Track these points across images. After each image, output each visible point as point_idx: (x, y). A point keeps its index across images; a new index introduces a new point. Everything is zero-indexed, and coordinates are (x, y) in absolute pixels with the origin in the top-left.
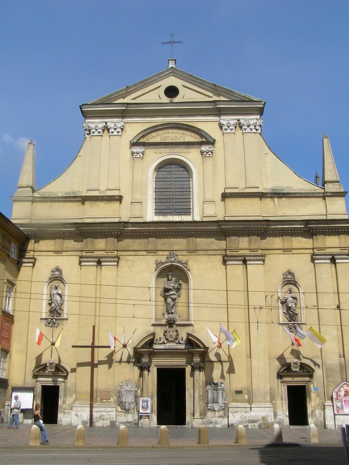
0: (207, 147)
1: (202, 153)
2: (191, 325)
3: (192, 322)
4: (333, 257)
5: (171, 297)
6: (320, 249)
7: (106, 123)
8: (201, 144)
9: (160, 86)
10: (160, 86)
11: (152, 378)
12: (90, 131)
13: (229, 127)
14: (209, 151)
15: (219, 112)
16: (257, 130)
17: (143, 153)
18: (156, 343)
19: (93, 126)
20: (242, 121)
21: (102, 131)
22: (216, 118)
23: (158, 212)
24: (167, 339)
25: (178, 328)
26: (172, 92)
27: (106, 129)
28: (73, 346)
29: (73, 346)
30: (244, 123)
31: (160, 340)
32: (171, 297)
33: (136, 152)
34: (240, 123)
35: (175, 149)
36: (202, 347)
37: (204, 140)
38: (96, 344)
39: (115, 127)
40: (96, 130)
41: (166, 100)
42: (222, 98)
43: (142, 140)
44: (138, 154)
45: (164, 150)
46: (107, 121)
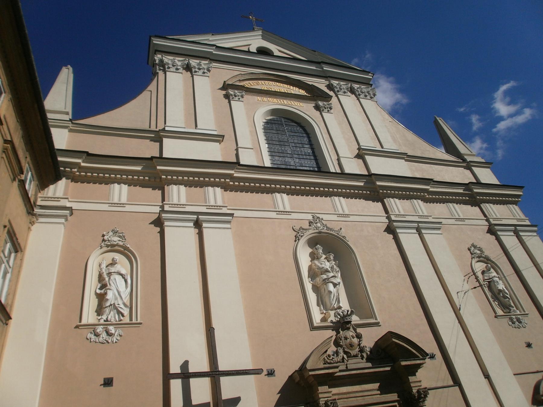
3: (379, 320)
5: (332, 282)
18: (329, 361)
24: (345, 352)
25: (359, 330)
32: (332, 282)
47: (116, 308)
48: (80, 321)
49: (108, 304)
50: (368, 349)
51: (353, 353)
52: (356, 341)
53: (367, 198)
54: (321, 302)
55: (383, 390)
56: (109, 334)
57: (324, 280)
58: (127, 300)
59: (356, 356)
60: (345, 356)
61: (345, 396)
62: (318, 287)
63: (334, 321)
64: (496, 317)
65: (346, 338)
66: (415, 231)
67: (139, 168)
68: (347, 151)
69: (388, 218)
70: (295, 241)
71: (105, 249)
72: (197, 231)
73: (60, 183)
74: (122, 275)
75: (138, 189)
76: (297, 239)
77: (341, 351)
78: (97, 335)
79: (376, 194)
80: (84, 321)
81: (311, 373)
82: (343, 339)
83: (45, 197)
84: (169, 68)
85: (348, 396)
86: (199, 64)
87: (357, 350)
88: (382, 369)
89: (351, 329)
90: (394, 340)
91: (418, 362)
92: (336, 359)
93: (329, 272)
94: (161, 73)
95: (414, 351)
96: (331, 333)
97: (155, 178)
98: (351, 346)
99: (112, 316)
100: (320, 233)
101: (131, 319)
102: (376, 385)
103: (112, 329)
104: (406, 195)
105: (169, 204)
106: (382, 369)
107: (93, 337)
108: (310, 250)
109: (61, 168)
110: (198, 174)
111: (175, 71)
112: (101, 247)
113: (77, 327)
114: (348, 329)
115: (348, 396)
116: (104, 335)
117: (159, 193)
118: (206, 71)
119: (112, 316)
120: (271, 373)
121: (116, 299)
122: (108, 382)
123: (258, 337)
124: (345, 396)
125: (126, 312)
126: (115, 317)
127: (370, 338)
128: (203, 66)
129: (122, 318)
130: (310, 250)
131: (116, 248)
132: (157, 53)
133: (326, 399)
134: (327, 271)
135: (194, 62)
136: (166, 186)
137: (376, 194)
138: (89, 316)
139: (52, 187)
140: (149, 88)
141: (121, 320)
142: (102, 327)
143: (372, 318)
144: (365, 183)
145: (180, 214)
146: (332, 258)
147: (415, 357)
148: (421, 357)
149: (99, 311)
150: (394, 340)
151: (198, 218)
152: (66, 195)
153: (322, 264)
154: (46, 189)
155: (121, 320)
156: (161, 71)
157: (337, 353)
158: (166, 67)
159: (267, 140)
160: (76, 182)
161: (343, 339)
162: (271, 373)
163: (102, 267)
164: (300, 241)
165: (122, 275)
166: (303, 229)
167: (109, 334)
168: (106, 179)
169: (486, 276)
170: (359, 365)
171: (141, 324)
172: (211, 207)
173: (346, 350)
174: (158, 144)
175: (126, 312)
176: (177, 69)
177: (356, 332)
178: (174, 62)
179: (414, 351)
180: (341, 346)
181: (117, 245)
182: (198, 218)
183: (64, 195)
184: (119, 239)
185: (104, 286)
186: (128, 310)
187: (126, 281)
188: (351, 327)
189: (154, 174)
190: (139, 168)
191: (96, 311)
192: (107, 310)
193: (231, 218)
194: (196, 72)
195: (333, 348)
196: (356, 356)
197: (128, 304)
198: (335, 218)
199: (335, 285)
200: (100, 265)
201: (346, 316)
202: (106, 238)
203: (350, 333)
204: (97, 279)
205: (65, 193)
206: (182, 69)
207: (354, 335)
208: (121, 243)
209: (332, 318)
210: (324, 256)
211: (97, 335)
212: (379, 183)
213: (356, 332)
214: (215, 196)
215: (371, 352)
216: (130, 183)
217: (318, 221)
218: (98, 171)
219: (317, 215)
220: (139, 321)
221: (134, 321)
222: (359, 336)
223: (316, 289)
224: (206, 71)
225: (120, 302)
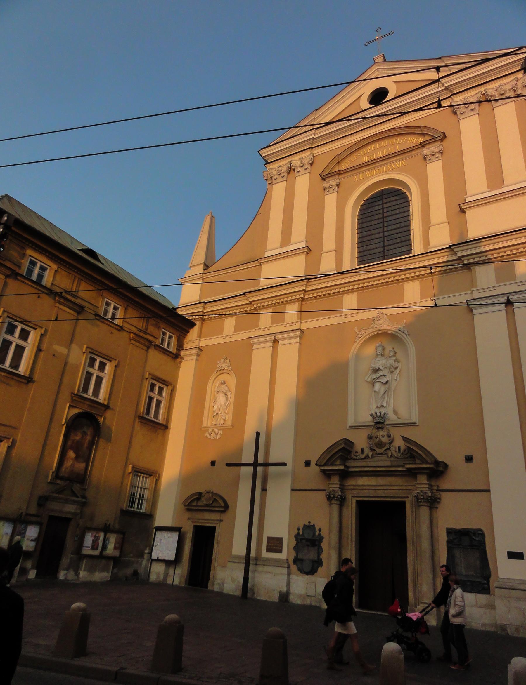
0: (432, 148)
7: (290, 164)
8: (423, 145)
12: (271, 178)
14: (435, 153)
18: (355, 457)
19: (275, 172)
21: (286, 176)
28: (228, 465)
29: (228, 465)
37: (427, 138)
39: (302, 165)
66: (503, 307)
196: (382, 454)
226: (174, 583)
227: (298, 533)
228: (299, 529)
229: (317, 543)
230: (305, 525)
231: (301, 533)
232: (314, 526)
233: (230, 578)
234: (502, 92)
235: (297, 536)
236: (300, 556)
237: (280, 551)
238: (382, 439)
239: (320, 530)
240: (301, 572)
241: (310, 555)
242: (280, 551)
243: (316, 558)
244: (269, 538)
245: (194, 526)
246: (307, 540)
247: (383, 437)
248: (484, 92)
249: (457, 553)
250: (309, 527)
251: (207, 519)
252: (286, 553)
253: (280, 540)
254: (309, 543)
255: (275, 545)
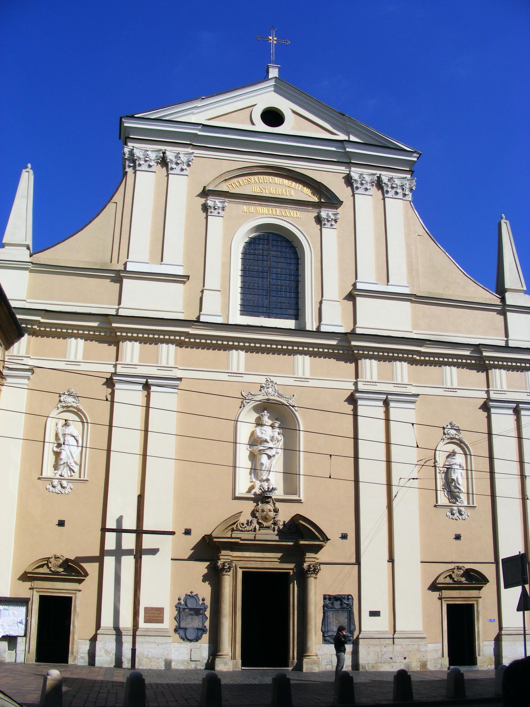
1: (319, 220)
2: (299, 501)
3: (302, 498)
4: (517, 406)
6: (502, 392)
9: (255, 105)
10: (255, 105)
11: (231, 587)
12: (134, 161)
13: (362, 184)
14: (332, 220)
15: (347, 160)
16: (405, 195)
17: (223, 209)
18: (241, 529)
20: (385, 179)
22: (343, 169)
23: (247, 308)
24: (259, 523)
25: (278, 505)
26: (272, 117)
27: (164, 162)
30: (386, 182)
31: (247, 524)
33: (214, 207)
34: (382, 181)
35: (278, 210)
36: (321, 539)
38: (146, 527)
40: (146, 161)
41: (261, 126)
42: (353, 138)
43: (224, 187)
44: (215, 209)
45: (260, 209)
46: (165, 150)
47: (68, 466)
48: (42, 475)
49: (62, 462)
50: (281, 523)
51: (265, 524)
52: (272, 514)
53: (338, 358)
54: (255, 470)
55: (282, 560)
56: (63, 487)
57: (260, 450)
58: (77, 459)
59: (268, 527)
60: (257, 527)
61: (246, 559)
62: (255, 455)
63: (258, 493)
64: (435, 506)
65: (263, 511)
67: (95, 324)
68: (335, 289)
69: (356, 384)
70: (241, 407)
71: (61, 410)
72: (145, 393)
73: (23, 338)
74: (74, 437)
75: (95, 344)
76: (242, 406)
77: (255, 521)
78: (54, 487)
79: (351, 353)
80: (44, 475)
81: (215, 540)
82: (260, 511)
83: (11, 356)
84: (140, 165)
85: (249, 559)
86: (177, 156)
87: (272, 522)
88: (284, 543)
89: (271, 503)
90: (301, 521)
91: (320, 543)
92: (248, 528)
93: (268, 442)
94: (130, 171)
95: (317, 533)
96: (251, 506)
97: (111, 333)
98: (266, 519)
99: (66, 473)
100: (268, 400)
101: (80, 477)
102: (279, 555)
103: (65, 483)
104: (386, 357)
105: (122, 364)
106: (284, 543)
107: (51, 489)
108: (257, 415)
109: (23, 326)
110: (154, 331)
111: (147, 169)
112: (58, 409)
113: (39, 478)
114: (268, 503)
115: (249, 559)
116: (59, 487)
117: (113, 348)
118: (185, 167)
119: (66, 473)
120: (188, 532)
121: (68, 458)
122: (61, 523)
123: (183, 500)
124: (246, 559)
125: (76, 468)
126: (67, 473)
127: (285, 514)
128: (182, 159)
129: (73, 474)
130: (257, 415)
131: (71, 409)
132: (128, 140)
133: (225, 560)
134: (266, 441)
135: (171, 153)
136: (121, 343)
137: (351, 353)
138: (48, 471)
139: (16, 345)
140: (114, 199)
141: (72, 476)
142: (57, 480)
143: (295, 494)
144: (339, 341)
145: (130, 379)
146: (277, 425)
147: (318, 539)
148: (321, 539)
149: (56, 467)
150: (301, 521)
151: (147, 382)
152: (29, 354)
153: (262, 433)
154: (12, 348)
155: (72, 476)
156: (131, 168)
157: (249, 523)
158: (137, 163)
159: (244, 270)
160: (37, 336)
161: (260, 511)
162: (188, 532)
163: (58, 427)
164: (245, 408)
165: (74, 437)
166: (251, 394)
167: (63, 487)
168: (63, 335)
169: (448, 462)
170: (270, 536)
171: (87, 481)
172: (162, 368)
173: (260, 521)
174: (118, 285)
175: (76, 468)
176: (150, 166)
177: (274, 506)
178: (146, 156)
179: (317, 533)
180: (256, 517)
181: (72, 406)
182: (147, 382)
183: (26, 353)
184: (73, 400)
185: (59, 445)
186: (78, 467)
187: (77, 441)
188: (271, 501)
189: (109, 330)
190: (95, 324)
191: (54, 467)
192: (62, 467)
193: (179, 382)
194: (172, 169)
195: (250, 518)
196: (268, 527)
197: (79, 463)
198: (291, 382)
199: (269, 457)
200: (57, 425)
201: (266, 491)
202: (62, 399)
203: (270, 507)
204: (55, 438)
205: (27, 352)
206: (156, 164)
207: (272, 509)
208: (75, 405)
209: (257, 490)
210: (270, 422)
211: (54, 487)
212: (353, 343)
213: (274, 506)
214: (168, 353)
215: (284, 524)
216: (86, 338)
217: (270, 386)
218: (58, 325)
219: (271, 377)
220: (86, 479)
221: (82, 478)
222: (276, 511)
223: (253, 457)
224: (185, 167)
225: (72, 461)
226: (18, 661)
227: (179, 603)
228: (179, 599)
229: (201, 612)
230: (186, 595)
231: (183, 603)
232: (197, 595)
233: (103, 651)
234: (395, 186)
235: (178, 607)
236: (183, 625)
237: (161, 621)
238: (269, 513)
239: (203, 600)
240: (184, 640)
241: (194, 623)
242: (161, 621)
243: (200, 626)
244: (146, 609)
245: (40, 596)
246: (191, 609)
247: (270, 511)
248: (378, 175)
249: (330, 614)
250: (191, 596)
251: (59, 588)
252: (169, 621)
253: (160, 611)
254: (192, 612)
255: (155, 615)
